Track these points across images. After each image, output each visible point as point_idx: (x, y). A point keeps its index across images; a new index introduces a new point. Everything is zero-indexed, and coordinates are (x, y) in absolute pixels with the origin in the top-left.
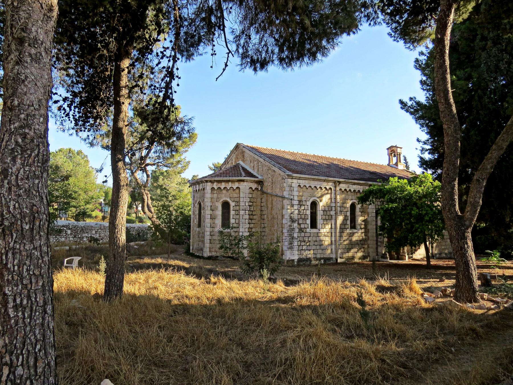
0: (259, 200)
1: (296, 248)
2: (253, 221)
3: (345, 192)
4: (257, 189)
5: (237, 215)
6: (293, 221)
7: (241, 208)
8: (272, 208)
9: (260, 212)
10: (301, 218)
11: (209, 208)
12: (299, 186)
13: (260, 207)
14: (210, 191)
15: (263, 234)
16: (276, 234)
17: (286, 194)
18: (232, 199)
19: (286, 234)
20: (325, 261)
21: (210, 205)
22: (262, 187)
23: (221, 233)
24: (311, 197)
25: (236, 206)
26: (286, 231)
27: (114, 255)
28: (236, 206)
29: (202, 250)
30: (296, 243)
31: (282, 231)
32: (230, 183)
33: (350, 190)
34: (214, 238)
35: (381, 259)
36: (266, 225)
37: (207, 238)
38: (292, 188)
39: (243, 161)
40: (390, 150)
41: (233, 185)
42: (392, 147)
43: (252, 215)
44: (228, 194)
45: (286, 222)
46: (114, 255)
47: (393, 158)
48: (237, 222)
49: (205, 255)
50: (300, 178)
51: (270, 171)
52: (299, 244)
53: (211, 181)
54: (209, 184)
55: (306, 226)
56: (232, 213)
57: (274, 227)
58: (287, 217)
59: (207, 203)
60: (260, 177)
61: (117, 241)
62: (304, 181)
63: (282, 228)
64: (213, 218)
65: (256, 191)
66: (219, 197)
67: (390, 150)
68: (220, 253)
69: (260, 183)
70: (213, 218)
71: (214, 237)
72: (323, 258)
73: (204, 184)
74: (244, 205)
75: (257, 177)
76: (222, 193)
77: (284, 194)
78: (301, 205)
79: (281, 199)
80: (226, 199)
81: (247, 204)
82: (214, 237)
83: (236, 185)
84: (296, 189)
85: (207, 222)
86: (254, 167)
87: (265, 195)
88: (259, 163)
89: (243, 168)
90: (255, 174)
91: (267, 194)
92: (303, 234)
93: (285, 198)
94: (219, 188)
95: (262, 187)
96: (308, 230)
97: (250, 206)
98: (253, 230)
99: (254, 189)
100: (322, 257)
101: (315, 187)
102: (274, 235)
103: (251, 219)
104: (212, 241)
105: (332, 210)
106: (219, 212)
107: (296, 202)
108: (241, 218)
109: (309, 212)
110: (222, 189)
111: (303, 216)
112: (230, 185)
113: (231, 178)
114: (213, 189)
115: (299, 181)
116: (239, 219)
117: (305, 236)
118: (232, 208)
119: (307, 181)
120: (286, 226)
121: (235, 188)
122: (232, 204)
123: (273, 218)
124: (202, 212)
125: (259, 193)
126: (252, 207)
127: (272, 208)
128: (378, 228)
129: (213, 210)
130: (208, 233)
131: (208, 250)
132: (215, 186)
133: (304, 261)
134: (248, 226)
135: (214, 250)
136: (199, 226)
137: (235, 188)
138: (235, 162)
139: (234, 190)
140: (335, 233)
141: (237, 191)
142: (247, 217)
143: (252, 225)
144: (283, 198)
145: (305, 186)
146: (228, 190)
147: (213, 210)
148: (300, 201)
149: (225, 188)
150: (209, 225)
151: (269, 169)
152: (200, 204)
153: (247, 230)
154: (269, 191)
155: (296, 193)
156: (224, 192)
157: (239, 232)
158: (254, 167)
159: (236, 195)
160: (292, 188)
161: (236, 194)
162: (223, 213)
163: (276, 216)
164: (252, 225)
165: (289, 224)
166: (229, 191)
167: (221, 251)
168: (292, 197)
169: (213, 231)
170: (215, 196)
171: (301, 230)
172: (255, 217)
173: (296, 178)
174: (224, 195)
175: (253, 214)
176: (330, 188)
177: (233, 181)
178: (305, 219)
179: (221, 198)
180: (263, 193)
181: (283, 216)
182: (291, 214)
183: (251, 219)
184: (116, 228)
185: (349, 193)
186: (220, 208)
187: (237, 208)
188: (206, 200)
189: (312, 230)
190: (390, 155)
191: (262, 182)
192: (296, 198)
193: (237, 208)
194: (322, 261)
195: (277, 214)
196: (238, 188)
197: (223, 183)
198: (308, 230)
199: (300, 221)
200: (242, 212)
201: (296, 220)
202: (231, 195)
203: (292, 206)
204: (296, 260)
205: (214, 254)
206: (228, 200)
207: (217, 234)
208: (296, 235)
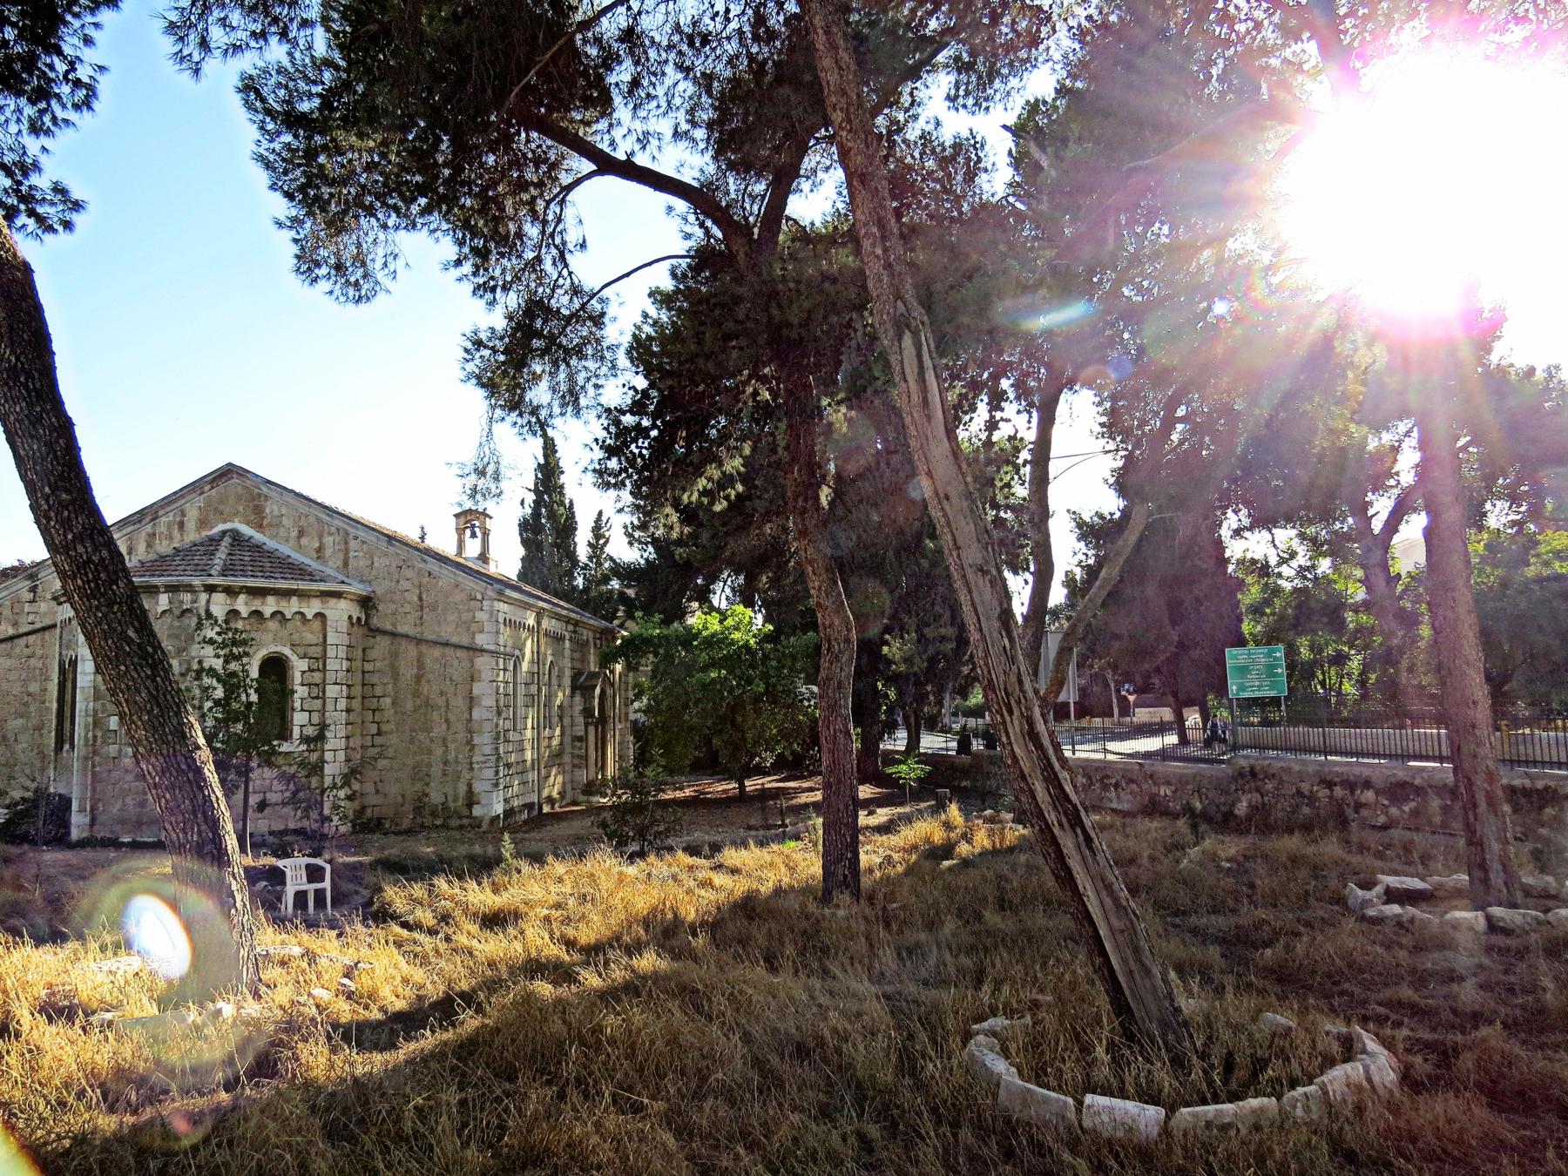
2: (352, 717)
5: (317, 698)
7: (330, 677)
8: (418, 678)
16: (439, 751)
18: (301, 650)
22: (368, 616)
25: (311, 670)
28: (311, 670)
31: (469, 742)
32: (294, 599)
36: (384, 727)
40: (462, 520)
41: (304, 604)
44: (285, 633)
48: (316, 718)
51: (409, 573)
54: (219, 598)
67: (462, 520)
76: (266, 630)
80: (279, 649)
87: (383, 643)
93: (482, 651)
94: (257, 614)
102: (430, 752)
108: (330, 706)
112: (292, 606)
116: (323, 711)
118: (298, 678)
122: (299, 666)
123: (427, 704)
127: (418, 678)
137: (309, 616)
141: (317, 625)
142: (342, 704)
149: (274, 614)
156: (273, 625)
158: (320, 550)
159: (310, 638)
163: (441, 701)
174: (271, 636)
177: (303, 595)
181: (471, 701)
187: (317, 677)
190: (460, 532)
193: (317, 677)
196: (320, 616)
197: (271, 599)
200: (332, 691)
206: (287, 651)
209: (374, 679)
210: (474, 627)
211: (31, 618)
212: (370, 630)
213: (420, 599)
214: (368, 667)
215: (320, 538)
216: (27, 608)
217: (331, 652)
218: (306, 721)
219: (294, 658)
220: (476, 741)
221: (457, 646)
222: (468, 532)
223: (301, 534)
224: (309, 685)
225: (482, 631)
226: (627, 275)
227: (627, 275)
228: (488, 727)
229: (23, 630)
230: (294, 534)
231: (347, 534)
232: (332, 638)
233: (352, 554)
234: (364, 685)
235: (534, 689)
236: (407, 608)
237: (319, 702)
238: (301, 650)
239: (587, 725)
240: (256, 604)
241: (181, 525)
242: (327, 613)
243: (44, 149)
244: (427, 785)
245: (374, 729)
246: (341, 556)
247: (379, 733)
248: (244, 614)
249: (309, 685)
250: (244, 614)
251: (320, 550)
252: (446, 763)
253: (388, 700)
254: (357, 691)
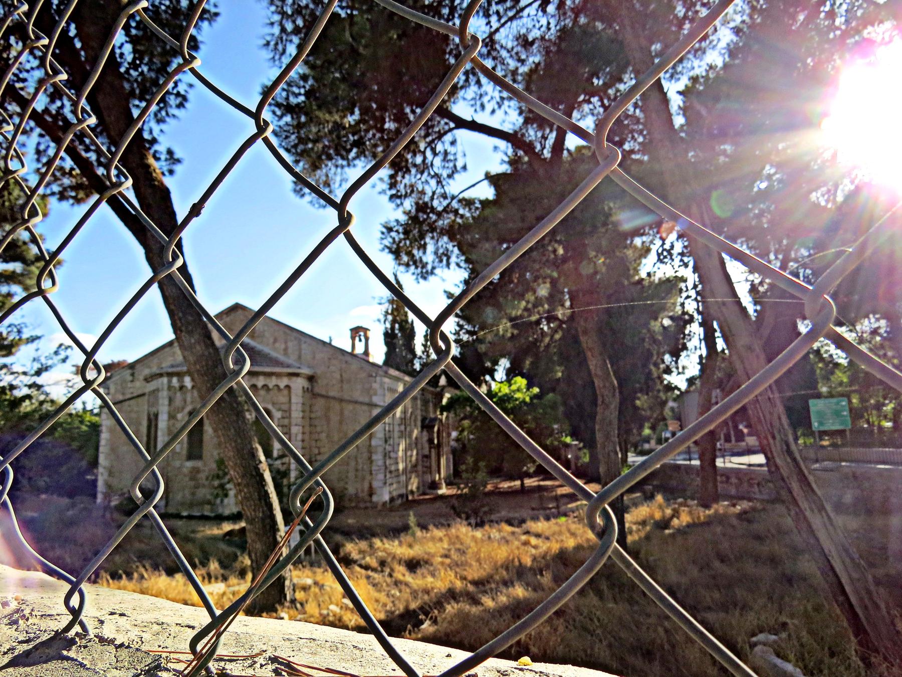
7: (294, 421)
25: (283, 418)
31: (370, 458)
32: (274, 378)
35: (428, 491)
36: (322, 450)
79: (365, 408)
83: (283, 382)
87: (321, 402)
141: (286, 392)
142: (300, 437)
158: (286, 350)
161: (284, 396)
166: (271, 392)
177: (278, 375)
190: (353, 338)
193: (286, 422)
196: (288, 387)
197: (261, 378)
209: (316, 422)
210: (372, 392)
211: (131, 390)
212: (314, 394)
213: (341, 376)
214: (313, 415)
215: (286, 342)
216: (129, 385)
217: (294, 407)
220: (374, 457)
221: (362, 403)
222: (357, 339)
223: (275, 341)
226: (474, 185)
227: (474, 185)
228: (380, 450)
229: (129, 396)
230: (271, 340)
232: (294, 400)
233: (303, 352)
235: (403, 428)
236: (334, 382)
238: (278, 407)
239: (430, 448)
242: (292, 385)
243: (162, 131)
244: (346, 483)
245: (316, 451)
246: (297, 353)
251: (286, 350)
252: (357, 470)
253: (323, 436)
254: (307, 429)
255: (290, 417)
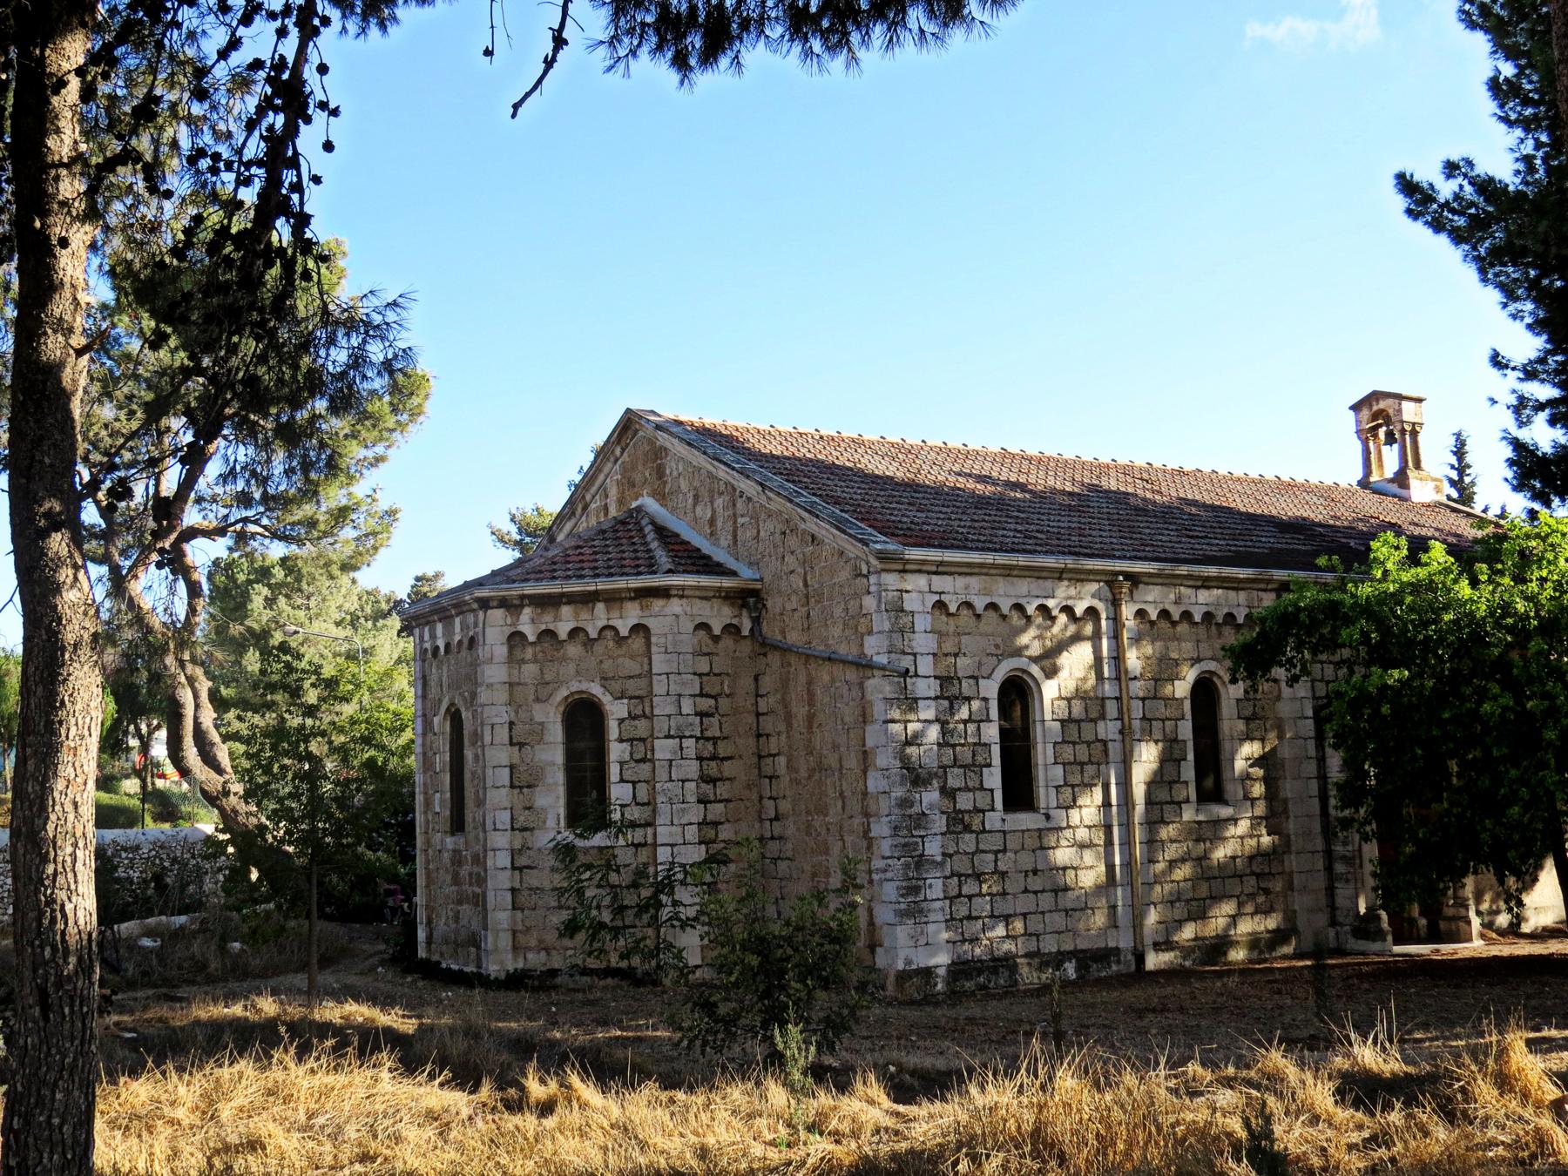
0: (746, 682)
1: (938, 911)
2: (723, 790)
3: (1164, 625)
4: (732, 630)
5: (643, 760)
6: (916, 777)
7: (661, 726)
8: (810, 719)
9: (752, 741)
10: (955, 764)
11: (503, 734)
12: (940, 605)
13: (751, 719)
14: (501, 651)
15: (773, 846)
16: (836, 849)
17: (875, 648)
19: (885, 847)
20: (1082, 967)
21: (506, 718)
22: (756, 621)
23: (566, 852)
24: (1000, 658)
25: (632, 717)
26: (886, 831)
27: (43, 994)
28: (632, 717)
29: (474, 941)
30: (935, 888)
31: (867, 831)
32: (600, 606)
33: (1187, 615)
34: (535, 883)
36: (785, 806)
37: (500, 881)
38: (906, 620)
39: (660, 496)
40: (1365, 414)
42: (1375, 396)
43: (714, 758)
45: (883, 785)
46: (43, 994)
47: (1385, 449)
49: (493, 969)
50: (940, 569)
51: (793, 541)
52: (954, 892)
53: (504, 603)
54: (497, 615)
55: (982, 800)
56: (616, 751)
57: (823, 810)
58: (885, 759)
59: (495, 710)
60: (746, 573)
61: (53, 921)
62: (961, 582)
63: (867, 815)
64: (523, 781)
65: (728, 642)
66: (548, 677)
67: (1365, 414)
68: (566, 955)
69: (748, 598)
70: (523, 781)
71: (533, 879)
72: (1074, 954)
73: (471, 618)
74: (670, 709)
75: (734, 574)
76: (564, 659)
77: (868, 651)
78: (952, 700)
79: (852, 675)
80: (584, 686)
81: (687, 707)
82: (533, 879)
83: (631, 615)
84: (922, 623)
85: (498, 801)
86: (712, 522)
87: (774, 659)
88: (740, 504)
89: (662, 532)
90: (720, 556)
91: (784, 650)
92: (968, 842)
94: (550, 633)
95: (756, 621)
96: (994, 820)
97: (702, 715)
98: (726, 833)
99: (717, 631)
100: (1068, 947)
101: (1019, 607)
102: (827, 852)
103: (713, 781)
104: (523, 898)
105: (1103, 716)
106: (552, 754)
107: (925, 687)
108: (662, 774)
109: (992, 732)
110: (563, 635)
111: (965, 755)
112: (600, 615)
113: (602, 585)
114: (516, 639)
115: (940, 582)
116: (651, 782)
117: (978, 851)
118: (613, 730)
119: (975, 582)
120: (884, 805)
121: (624, 632)
122: (615, 711)
123: (821, 768)
124: (469, 754)
125: (746, 647)
126: (715, 720)
127: (810, 719)
128: (1333, 792)
129: (521, 745)
130: (504, 860)
131: (505, 941)
132: (527, 624)
133: (980, 972)
134: (695, 813)
135: (533, 943)
136: (457, 824)
137: (624, 632)
138: (621, 501)
139: (620, 640)
140: (1127, 826)
141: (637, 643)
142: (692, 769)
143: (717, 810)
144: (865, 666)
145: (969, 605)
146: (589, 643)
147: (521, 745)
148: (945, 680)
149: (574, 633)
150: (504, 818)
151: (789, 529)
152: (455, 718)
153: (692, 833)
154: (794, 638)
155: (923, 642)
156: (573, 650)
157: (655, 845)
158: (712, 522)
159: (630, 666)
160: (906, 620)
161: (632, 657)
162: (572, 756)
163: (832, 760)
164: (717, 810)
165: (898, 792)
166: (599, 648)
167: (567, 942)
168: (906, 662)
169: (525, 848)
170: (530, 670)
171: (958, 823)
172: (728, 768)
173: (921, 568)
174: (572, 668)
175: (722, 753)
176: (1092, 612)
177: (613, 599)
178: (976, 767)
179: (559, 683)
180: (763, 645)
181: (866, 757)
182: (908, 743)
183: (713, 781)
184: (45, 859)
185: (1183, 628)
186: (556, 732)
187: (641, 728)
188: (484, 696)
189: (1009, 817)
190: (1366, 435)
191: (755, 593)
192: (925, 666)
193: (641, 728)
194: (1070, 969)
195: (835, 747)
196: (640, 629)
197: (566, 610)
198: (994, 820)
199: (954, 779)
200: (664, 749)
201: (931, 775)
202: (607, 665)
203: (911, 703)
204: (942, 972)
205: (536, 960)
206: (596, 689)
207: (550, 861)
208: (933, 848)
213: (806, 585)
214: (763, 708)
218: (628, 799)
219: (606, 699)
221: (845, 662)
224: (631, 740)
225: (870, 633)
231: (734, 489)
232: (659, 663)
234: (759, 736)
237: (646, 767)
240: (547, 622)
241: (606, 508)
242: (651, 623)
247: (777, 818)
248: (531, 638)
249: (631, 740)
250: (531, 638)
253: (782, 760)
255: (650, 717)
